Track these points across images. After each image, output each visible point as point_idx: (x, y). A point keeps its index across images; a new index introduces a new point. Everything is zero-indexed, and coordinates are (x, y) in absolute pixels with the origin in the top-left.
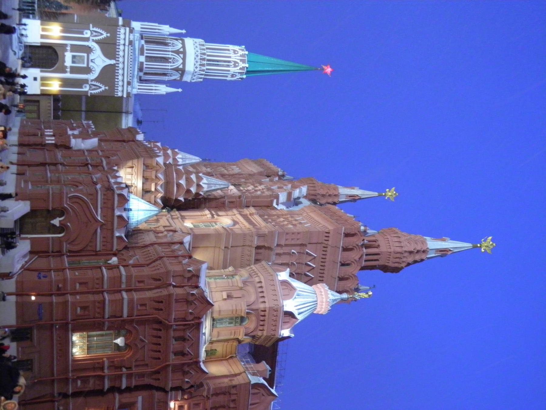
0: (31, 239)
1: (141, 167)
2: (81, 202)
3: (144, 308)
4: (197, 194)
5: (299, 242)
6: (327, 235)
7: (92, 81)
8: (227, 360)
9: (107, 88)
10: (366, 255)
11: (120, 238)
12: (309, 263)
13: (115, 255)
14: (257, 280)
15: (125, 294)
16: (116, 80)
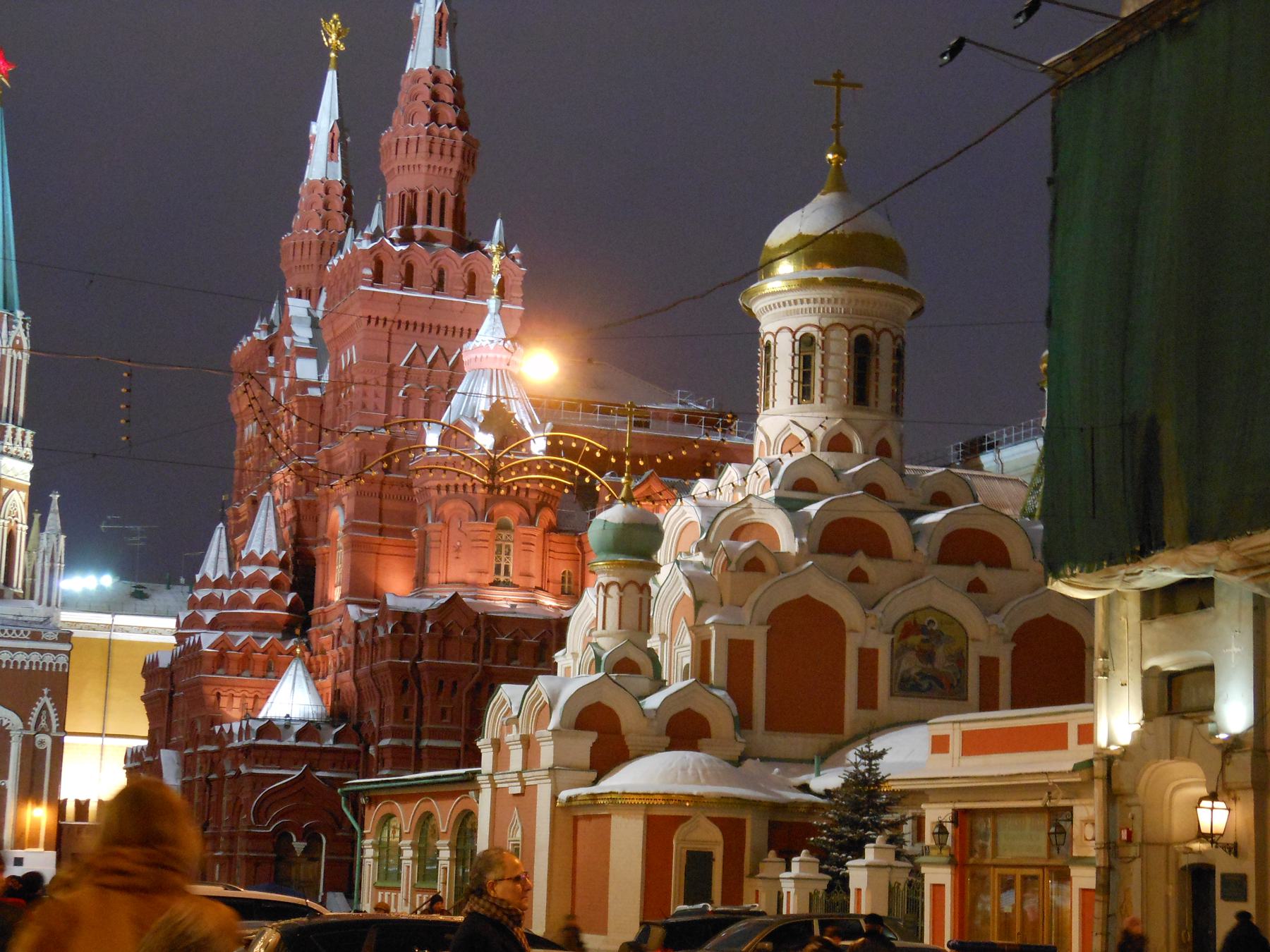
0: (325, 891)
1: (220, 676)
2: (266, 804)
3: (449, 713)
4: (283, 565)
5: (384, 381)
6: (373, 322)
7: (26, 727)
8: (584, 553)
9: (46, 691)
10: (429, 222)
11: (337, 739)
12: (429, 360)
13: (367, 749)
14: (434, 493)
15: (425, 743)
16: (26, 667)
